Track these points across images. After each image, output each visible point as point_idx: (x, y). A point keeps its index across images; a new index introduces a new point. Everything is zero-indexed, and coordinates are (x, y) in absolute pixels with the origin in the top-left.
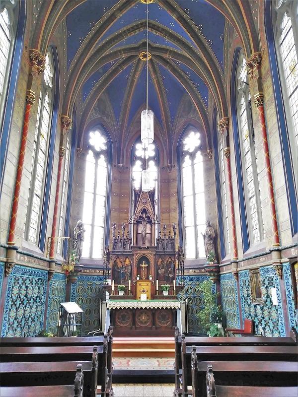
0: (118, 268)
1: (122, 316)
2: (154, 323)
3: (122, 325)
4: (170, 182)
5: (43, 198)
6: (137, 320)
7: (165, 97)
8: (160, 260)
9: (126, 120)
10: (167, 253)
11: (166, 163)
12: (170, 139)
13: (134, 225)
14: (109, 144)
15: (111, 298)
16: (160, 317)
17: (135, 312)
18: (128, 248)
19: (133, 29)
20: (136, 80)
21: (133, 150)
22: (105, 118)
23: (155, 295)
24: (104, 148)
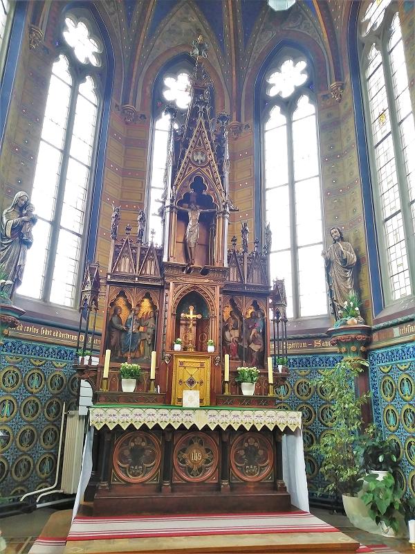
0: (120, 322)
1: (132, 450)
2: (224, 471)
6: (175, 461)
13: (171, 212)
14: (107, 55)
15: (96, 398)
16: (242, 453)
17: (169, 438)
23: (219, 397)
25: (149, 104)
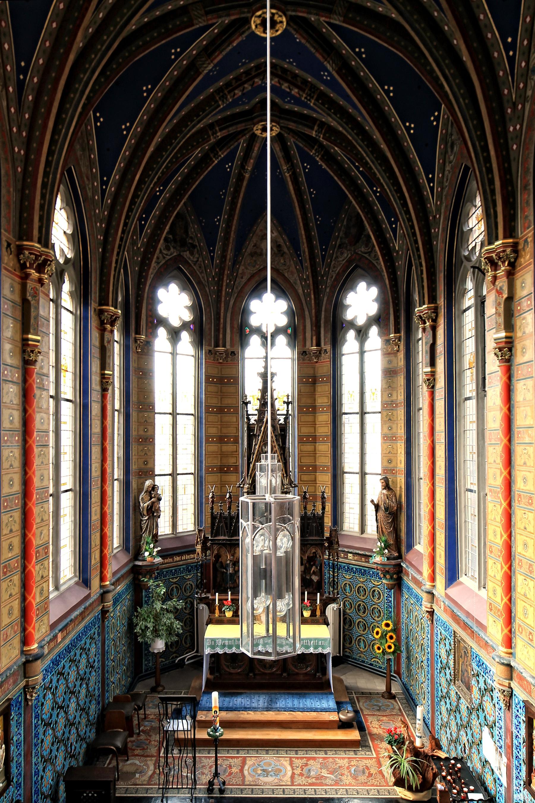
3: (232, 671)
4: (318, 377)
5: (78, 489)
7: (309, 206)
9: (230, 255)
11: (308, 343)
12: (317, 292)
14: (197, 308)
19: (239, 81)
20: (247, 176)
21: (245, 312)
22: (186, 254)
24: (188, 317)
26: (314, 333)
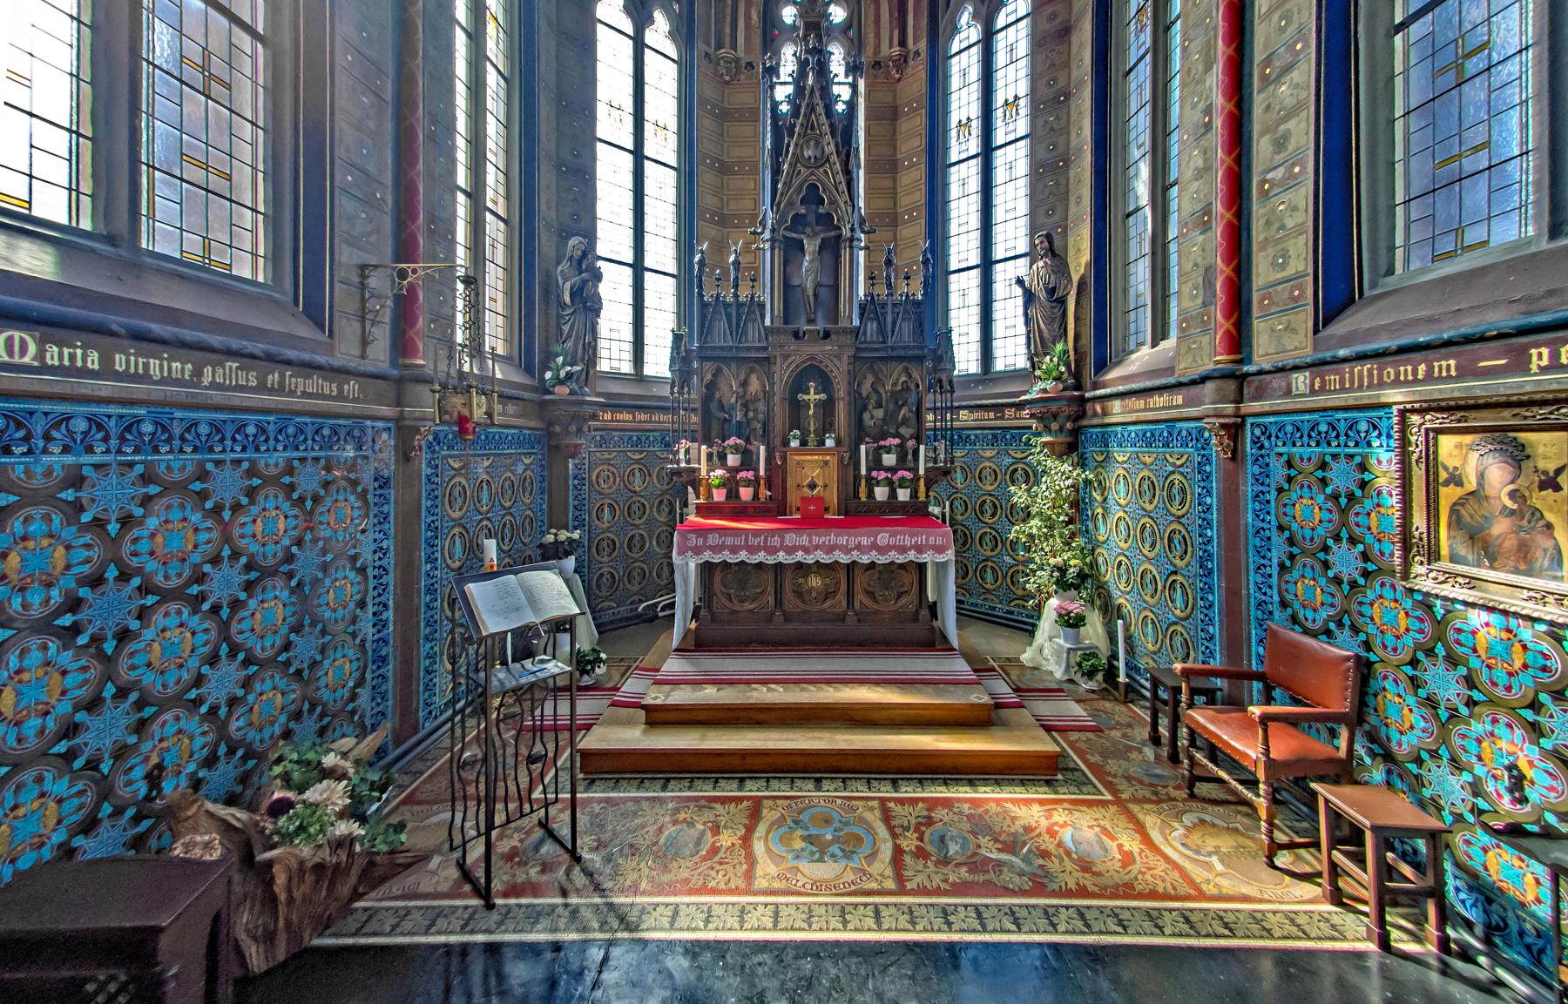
0: (722, 408)
8: (870, 379)
10: (895, 353)
13: (772, 249)
18: (753, 337)
25: (757, 38)
26: (895, 23)
